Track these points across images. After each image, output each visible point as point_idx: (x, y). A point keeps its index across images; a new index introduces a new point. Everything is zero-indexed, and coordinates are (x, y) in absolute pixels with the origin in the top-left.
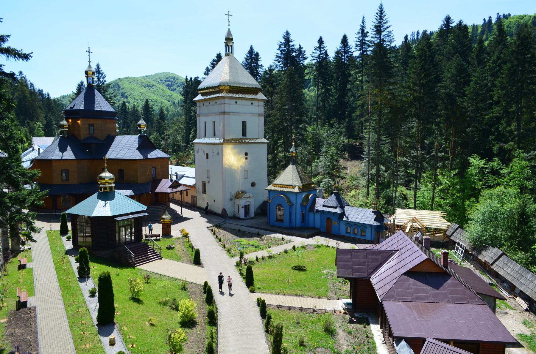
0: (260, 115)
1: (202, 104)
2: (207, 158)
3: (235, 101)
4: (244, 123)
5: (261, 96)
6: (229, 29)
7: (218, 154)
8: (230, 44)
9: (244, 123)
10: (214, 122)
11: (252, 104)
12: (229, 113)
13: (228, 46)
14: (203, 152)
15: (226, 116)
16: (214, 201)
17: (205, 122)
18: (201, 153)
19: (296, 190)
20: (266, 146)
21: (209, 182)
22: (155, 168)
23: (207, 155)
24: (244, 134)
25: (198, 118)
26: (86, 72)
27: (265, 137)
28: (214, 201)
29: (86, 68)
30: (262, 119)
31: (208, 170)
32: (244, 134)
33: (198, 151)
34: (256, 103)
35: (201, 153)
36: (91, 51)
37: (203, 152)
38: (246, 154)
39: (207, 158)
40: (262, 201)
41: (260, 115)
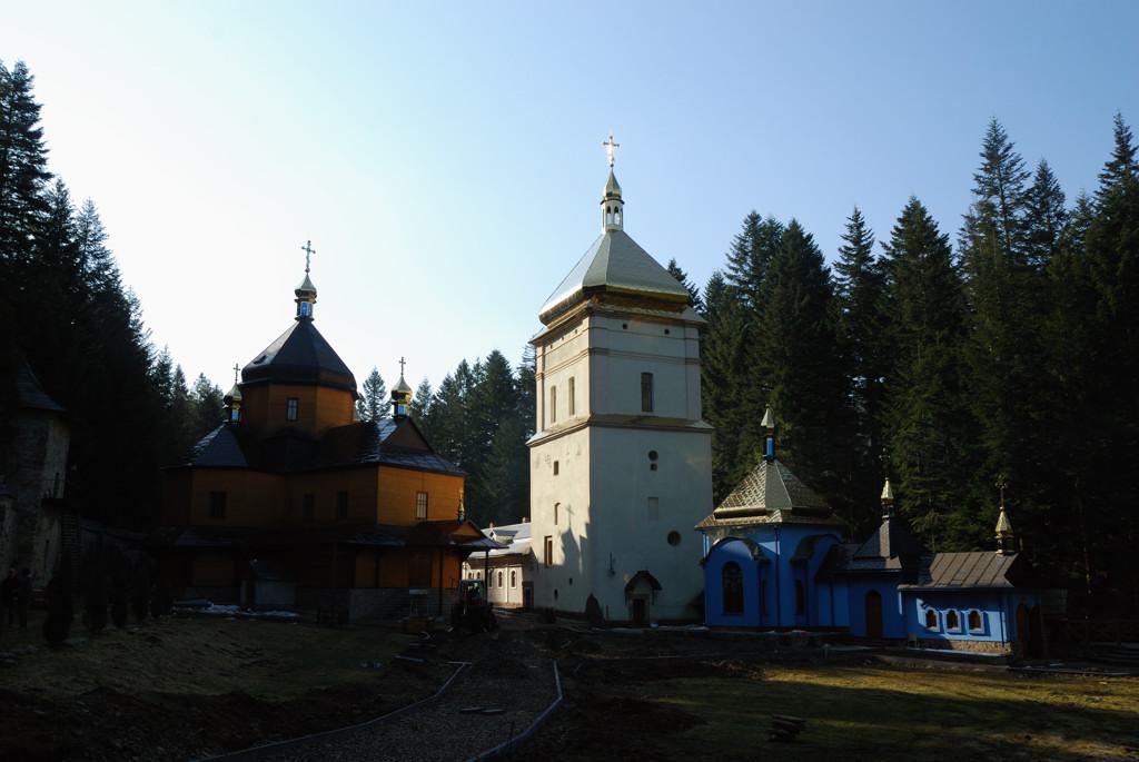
0: (688, 361)
2: (556, 472)
3: (620, 322)
4: (647, 380)
6: (613, 174)
7: (579, 454)
8: (612, 204)
9: (647, 380)
10: (572, 380)
11: (667, 332)
12: (605, 352)
15: (597, 357)
16: (571, 581)
17: (554, 389)
18: (543, 463)
19: (777, 517)
20: (706, 440)
22: (427, 494)
23: (556, 464)
24: (648, 403)
26: (298, 292)
27: (704, 417)
28: (571, 581)
29: (299, 284)
30: (696, 372)
31: (558, 504)
32: (648, 403)
33: (538, 463)
34: (676, 331)
35: (543, 463)
36: (312, 248)
38: (653, 455)
39: (556, 472)
41: (688, 361)
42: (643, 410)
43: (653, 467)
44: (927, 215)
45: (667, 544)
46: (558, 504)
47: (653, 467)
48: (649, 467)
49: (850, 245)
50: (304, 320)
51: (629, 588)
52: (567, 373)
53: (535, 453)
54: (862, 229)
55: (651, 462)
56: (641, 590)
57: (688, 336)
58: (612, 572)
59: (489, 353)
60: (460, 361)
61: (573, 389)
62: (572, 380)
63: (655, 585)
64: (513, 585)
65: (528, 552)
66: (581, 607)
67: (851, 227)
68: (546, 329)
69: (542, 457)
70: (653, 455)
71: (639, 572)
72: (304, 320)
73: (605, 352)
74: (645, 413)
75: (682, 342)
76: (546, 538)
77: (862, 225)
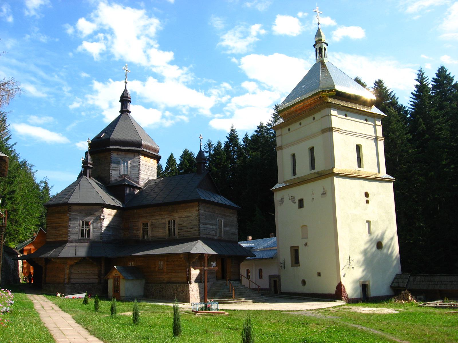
1: (285, 130)
4: (358, 148)
5: (375, 110)
7: (324, 193)
9: (358, 148)
10: (312, 150)
12: (338, 130)
13: (320, 49)
14: (293, 199)
16: (319, 274)
17: (294, 156)
18: (287, 202)
21: (306, 245)
25: (279, 153)
33: (282, 201)
37: (293, 199)
38: (367, 195)
42: (358, 167)
43: (367, 202)
44: (447, 73)
47: (367, 202)
49: (419, 84)
50: (124, 111)
52: (309, 144)
53: (277, 197)
54: (424, 76)
59: (183, 150)
60: (170, 153)
62: (312, 150)
64: (261, 276)
66: (333, 290)
67: (418, 74)
68: (281, 121)
69: (286, 199)
70: (367, 195)
72: (124, 111)
74: (359, 169)
76: (291, 247)
77: (423, 74)
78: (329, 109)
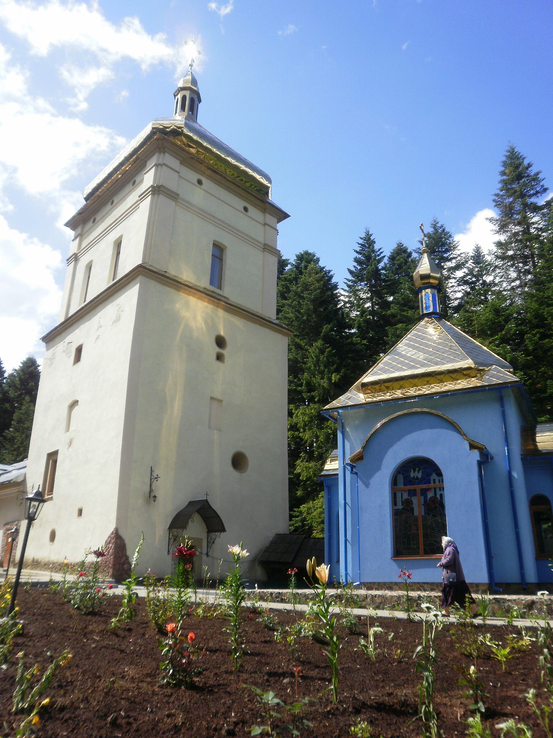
12: (173, 196)
40: (270, 535)
42: (212, 283)
45: (231, 468)
46: (75, 403)
48: (215, 357)
51: (179, 522)
55: (218, 350)
56: (195, 529)
57: (267, 222)
58: (151, 497)
61: (118, 253)
63: (213, 523)
65: (20, 480)
71: (191, 503)
73: (173, 196)
75: (261, 228)
78: (162, 154)
